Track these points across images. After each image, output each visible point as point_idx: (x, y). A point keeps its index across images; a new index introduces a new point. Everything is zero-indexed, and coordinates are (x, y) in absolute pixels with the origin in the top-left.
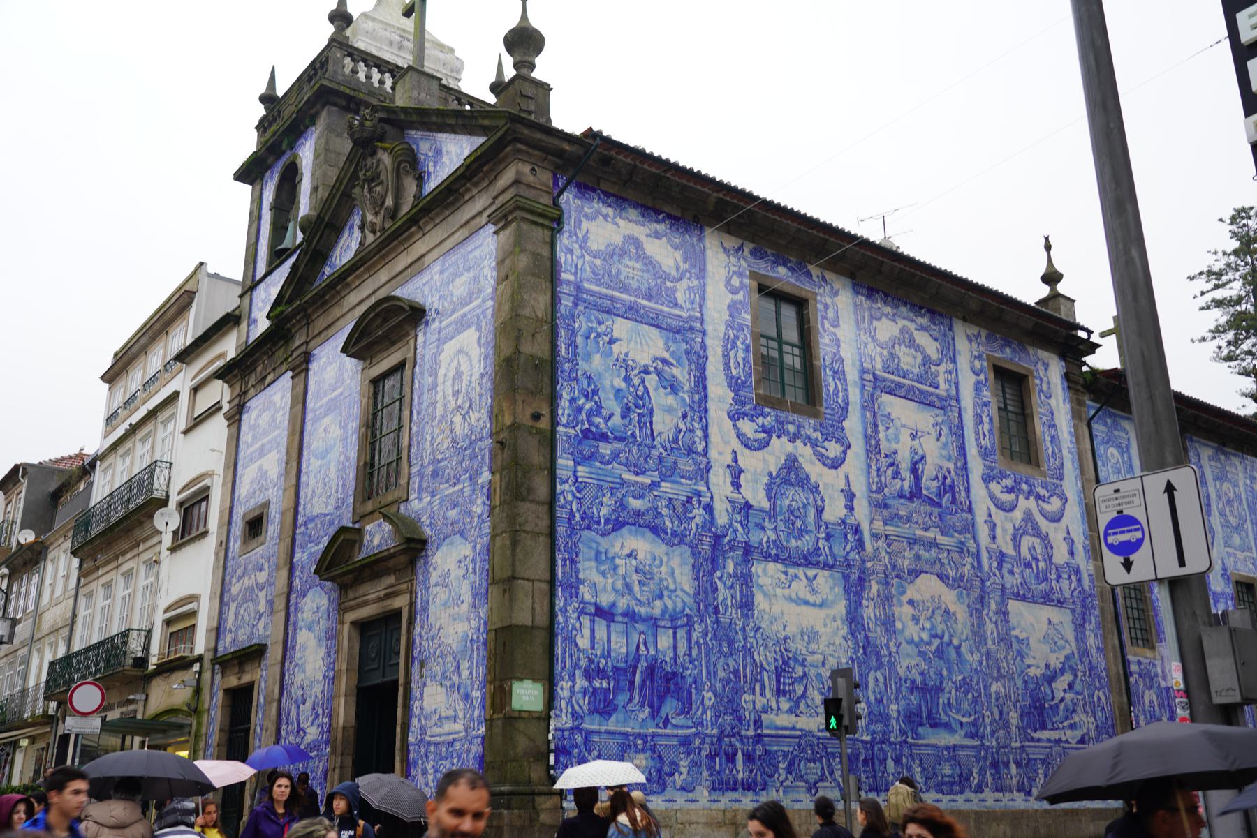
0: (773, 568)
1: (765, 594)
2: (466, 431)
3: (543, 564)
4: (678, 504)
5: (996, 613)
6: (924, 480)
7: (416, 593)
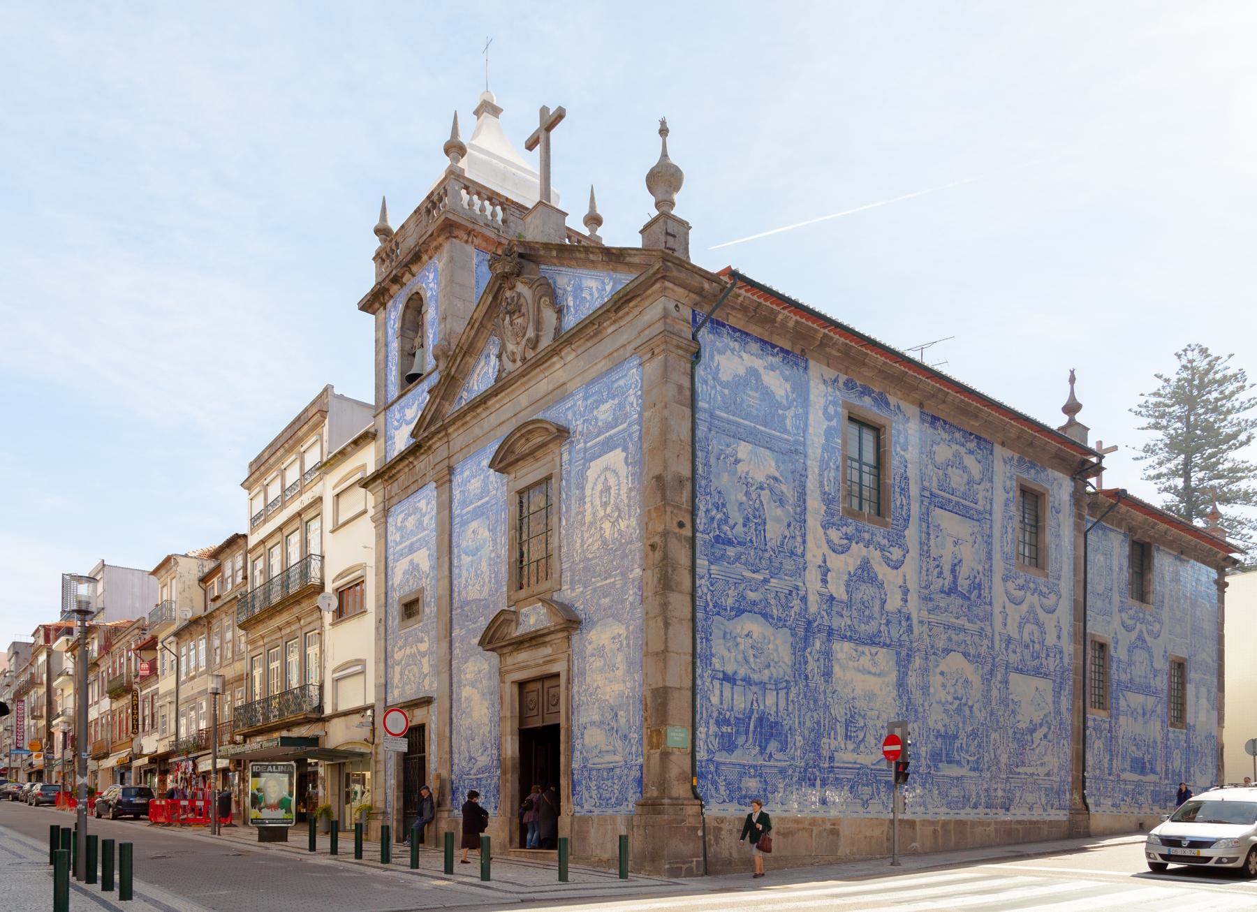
0: (847, 646)
1: (841, 666)
3: (689, 642)
4: (782, 596)
5: (1000, 682)
6: (960, 579)
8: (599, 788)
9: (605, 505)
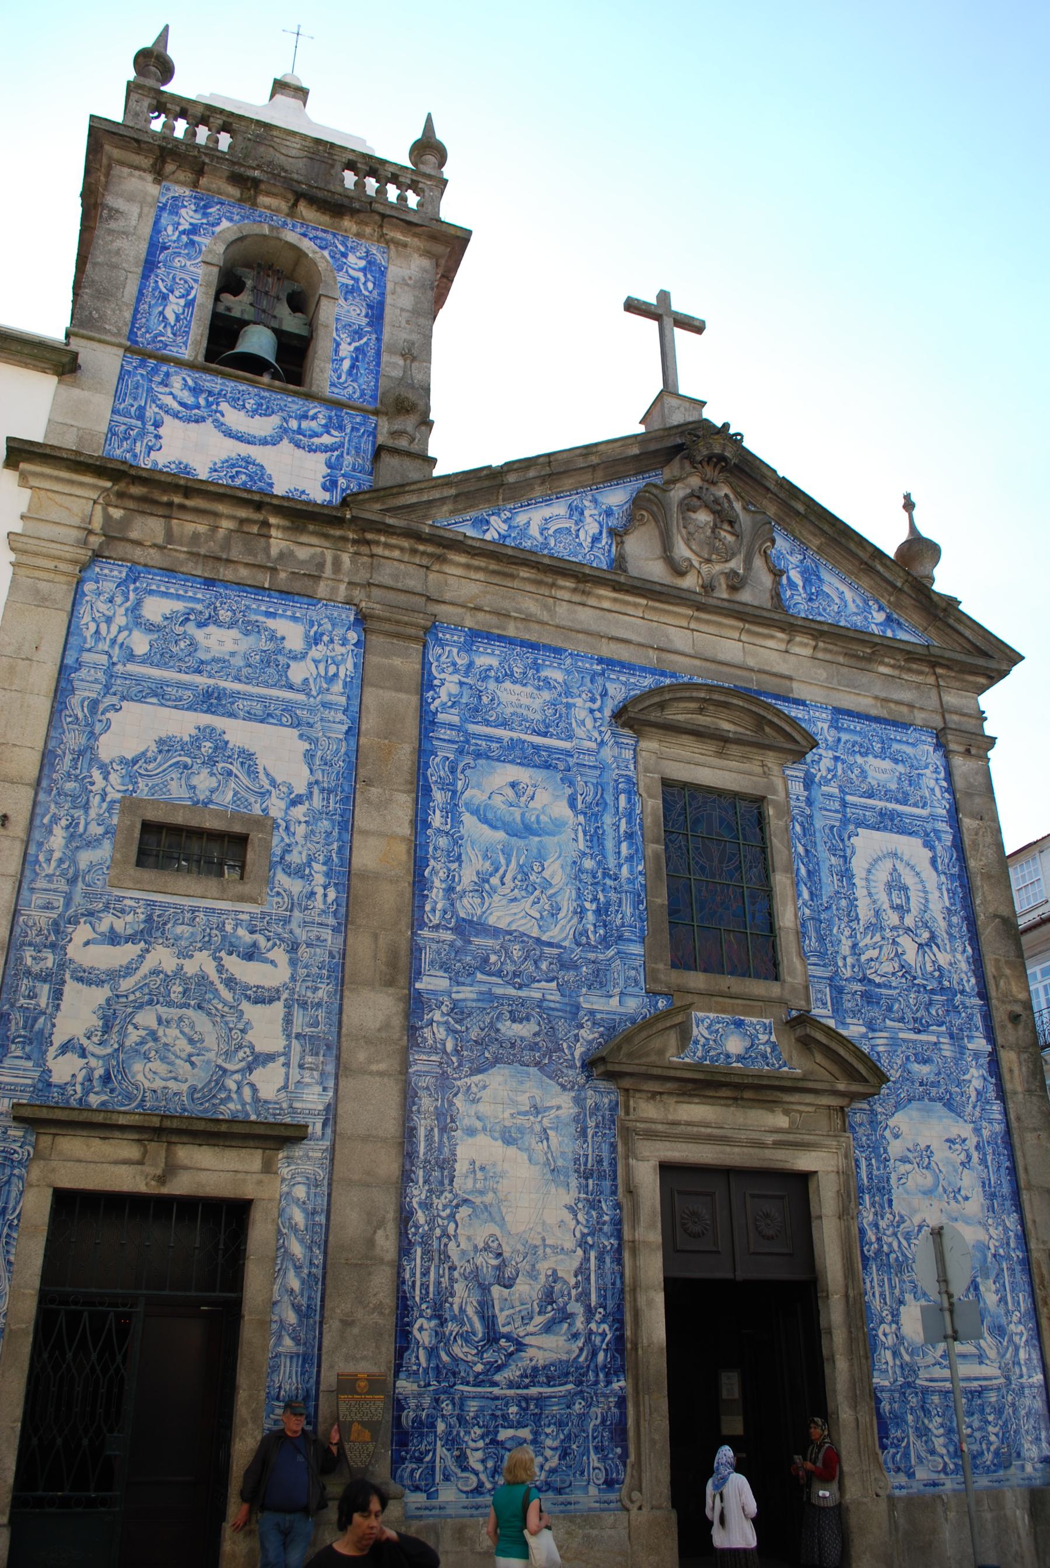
2: (929, 968)
7: (857, 1160)
8: (950, 1431)
9: (901, 910)
